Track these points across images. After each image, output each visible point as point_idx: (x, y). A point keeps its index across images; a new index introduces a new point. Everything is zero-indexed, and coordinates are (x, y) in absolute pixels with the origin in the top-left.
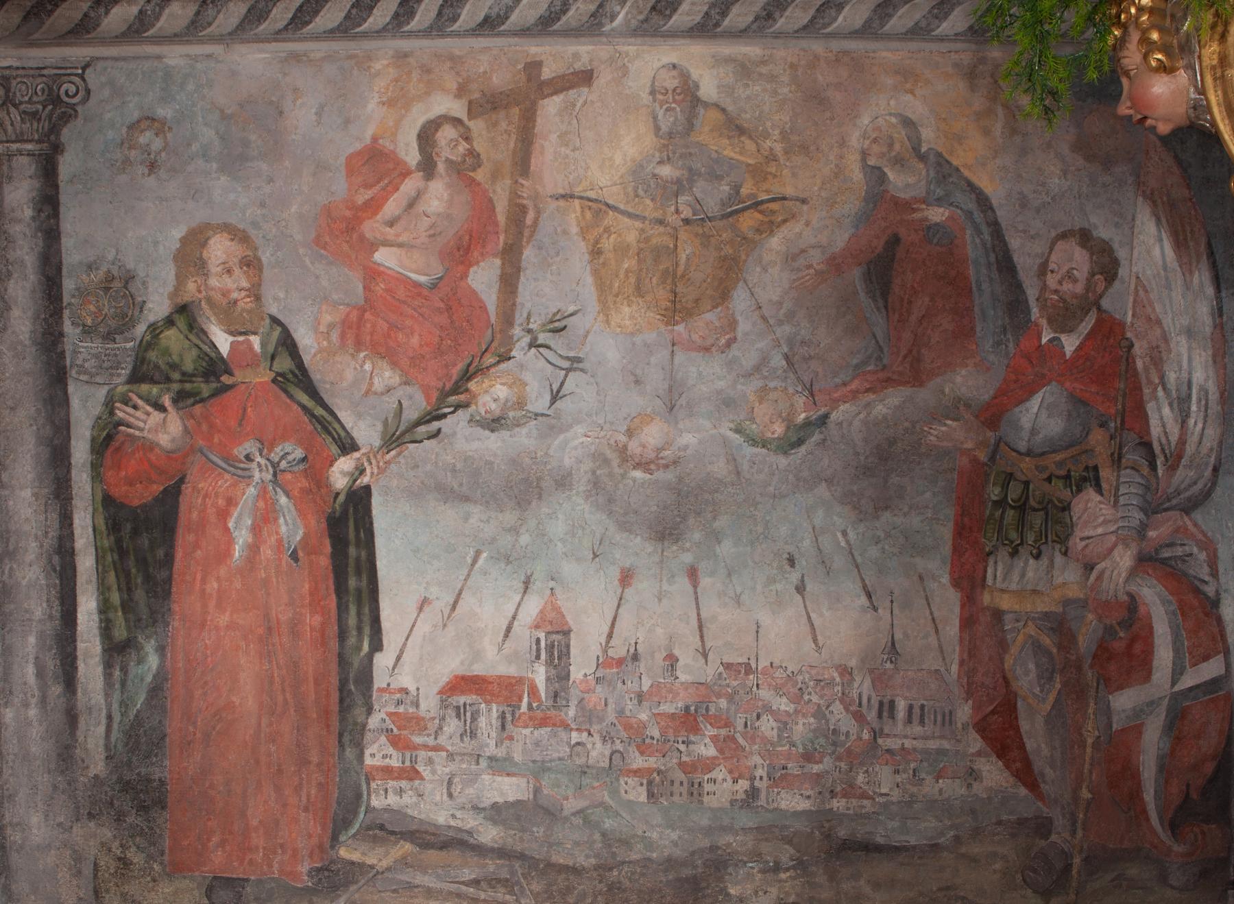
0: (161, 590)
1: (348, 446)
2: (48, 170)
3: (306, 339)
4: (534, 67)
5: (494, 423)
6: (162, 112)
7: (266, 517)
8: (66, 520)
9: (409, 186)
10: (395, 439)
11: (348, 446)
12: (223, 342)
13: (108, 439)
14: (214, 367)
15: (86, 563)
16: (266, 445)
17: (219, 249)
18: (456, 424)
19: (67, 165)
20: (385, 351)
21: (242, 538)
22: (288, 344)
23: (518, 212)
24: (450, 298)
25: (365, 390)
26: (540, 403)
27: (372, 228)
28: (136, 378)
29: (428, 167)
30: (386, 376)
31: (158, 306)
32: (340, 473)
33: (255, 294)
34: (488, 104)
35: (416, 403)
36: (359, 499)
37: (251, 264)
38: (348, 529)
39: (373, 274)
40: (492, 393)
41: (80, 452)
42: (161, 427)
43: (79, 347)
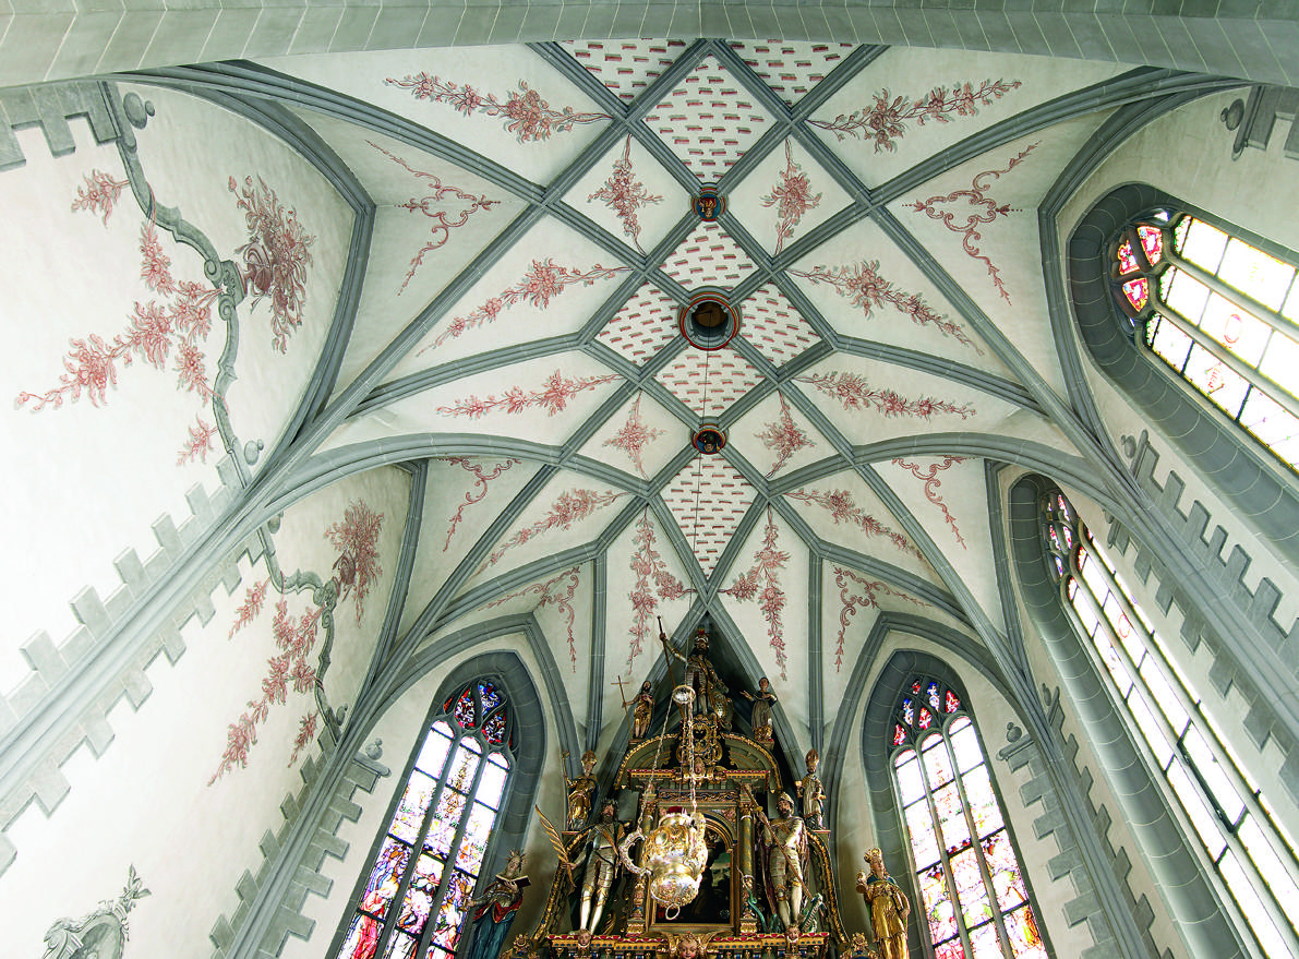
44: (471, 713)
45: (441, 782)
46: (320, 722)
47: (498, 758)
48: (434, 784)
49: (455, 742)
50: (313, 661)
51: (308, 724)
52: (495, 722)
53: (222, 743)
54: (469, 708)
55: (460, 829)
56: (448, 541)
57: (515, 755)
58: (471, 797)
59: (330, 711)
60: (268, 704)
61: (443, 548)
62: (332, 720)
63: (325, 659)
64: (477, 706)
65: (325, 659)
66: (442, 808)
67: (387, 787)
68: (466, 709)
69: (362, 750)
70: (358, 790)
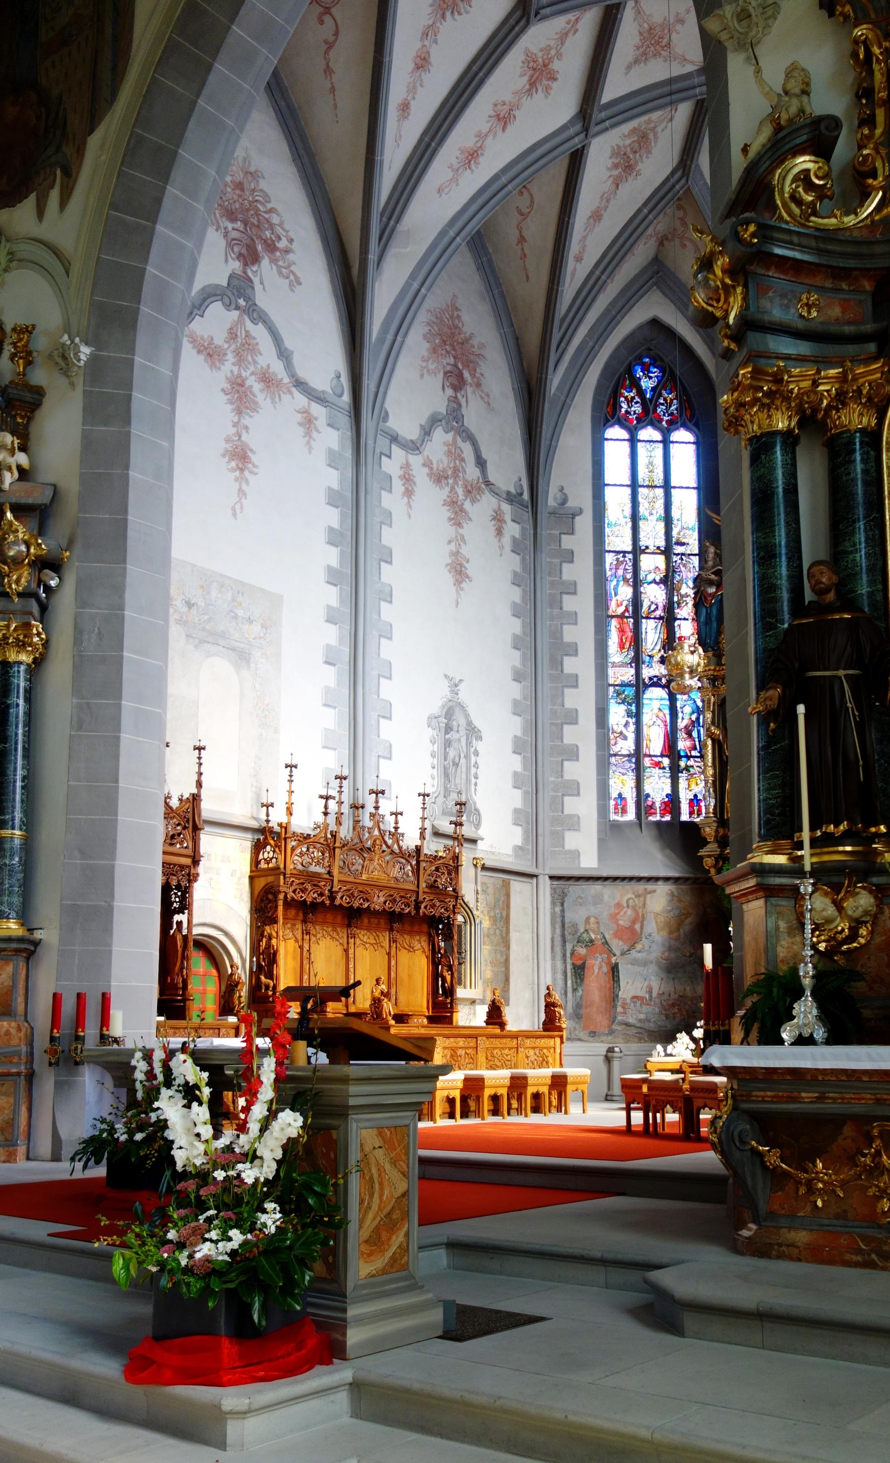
0: (582, 980)
1: (615, 955)
2: (562, 905)
3: (607, 937)
4: (646, 889)
5: (639, 952)
6: (583, 896)
7: (600, 968)
8: (566, 967)
9: (625, 909)
10: (623, 954)
11: (615, 955)
12: (593, 936)
13: (572, 954)
14: (592, 941)
15: (569, 974)
16: (601, 954)
17: (592, 920)
18: (633, 952)
19: (565, 905)
20: (621, 939)
21: (596, 971)
22: (604, 937)
23: (643, 915)
24: (631, 929)
25: (617, 946)
26: (647, 948)
27: (618, 917)
28: (578, 942)
29: (628, 906)
30: (621, 943)
31: (582, 930)
32: (613, 960)
33: (598, 928)
34: (638, 896)
35: (626, 948)
36: (617, 965)
37: (598, 923)
38: (614, 970)
39: (618, 925)
40: (639, 946)
41: (568, 955)
42: (582, 951)
43: (568, 937)
44: (637, 403)
45: (634, 485)
46: (506, 508)
47: (682, 435)
48: (628, 491)
49: (633, 441)
50: (472, 472)
51: (498, 518)
52: (665, 399)
53: (448, 578)
54: (633, 398)
55: (668, 520)
56: (525, 269)
57: (697, 425)
58: (667, 486)
59: (508, 493)
60: (461, 531)
61: (525, 279)
62: (511, 498)
63: (481, 463)
64: (641, 393)
65: (481, 463)
66: (643, 510)
67: (584, 524)
68: (630, 401)
69: (551, 502)
70: (563, 536)
